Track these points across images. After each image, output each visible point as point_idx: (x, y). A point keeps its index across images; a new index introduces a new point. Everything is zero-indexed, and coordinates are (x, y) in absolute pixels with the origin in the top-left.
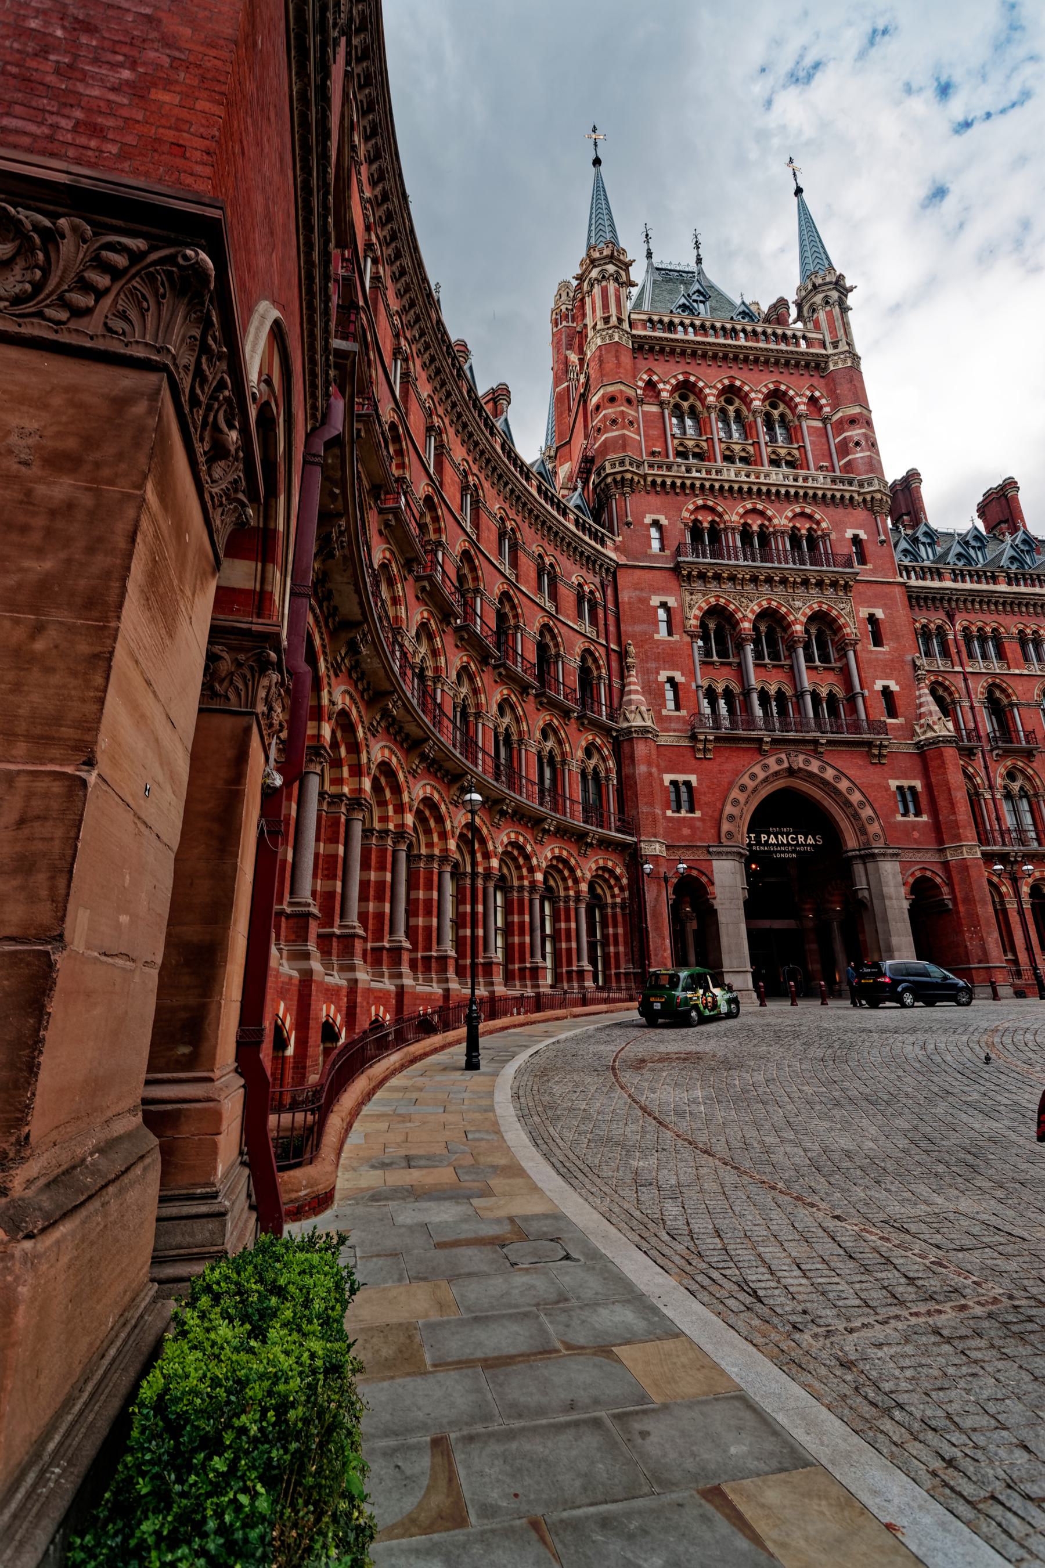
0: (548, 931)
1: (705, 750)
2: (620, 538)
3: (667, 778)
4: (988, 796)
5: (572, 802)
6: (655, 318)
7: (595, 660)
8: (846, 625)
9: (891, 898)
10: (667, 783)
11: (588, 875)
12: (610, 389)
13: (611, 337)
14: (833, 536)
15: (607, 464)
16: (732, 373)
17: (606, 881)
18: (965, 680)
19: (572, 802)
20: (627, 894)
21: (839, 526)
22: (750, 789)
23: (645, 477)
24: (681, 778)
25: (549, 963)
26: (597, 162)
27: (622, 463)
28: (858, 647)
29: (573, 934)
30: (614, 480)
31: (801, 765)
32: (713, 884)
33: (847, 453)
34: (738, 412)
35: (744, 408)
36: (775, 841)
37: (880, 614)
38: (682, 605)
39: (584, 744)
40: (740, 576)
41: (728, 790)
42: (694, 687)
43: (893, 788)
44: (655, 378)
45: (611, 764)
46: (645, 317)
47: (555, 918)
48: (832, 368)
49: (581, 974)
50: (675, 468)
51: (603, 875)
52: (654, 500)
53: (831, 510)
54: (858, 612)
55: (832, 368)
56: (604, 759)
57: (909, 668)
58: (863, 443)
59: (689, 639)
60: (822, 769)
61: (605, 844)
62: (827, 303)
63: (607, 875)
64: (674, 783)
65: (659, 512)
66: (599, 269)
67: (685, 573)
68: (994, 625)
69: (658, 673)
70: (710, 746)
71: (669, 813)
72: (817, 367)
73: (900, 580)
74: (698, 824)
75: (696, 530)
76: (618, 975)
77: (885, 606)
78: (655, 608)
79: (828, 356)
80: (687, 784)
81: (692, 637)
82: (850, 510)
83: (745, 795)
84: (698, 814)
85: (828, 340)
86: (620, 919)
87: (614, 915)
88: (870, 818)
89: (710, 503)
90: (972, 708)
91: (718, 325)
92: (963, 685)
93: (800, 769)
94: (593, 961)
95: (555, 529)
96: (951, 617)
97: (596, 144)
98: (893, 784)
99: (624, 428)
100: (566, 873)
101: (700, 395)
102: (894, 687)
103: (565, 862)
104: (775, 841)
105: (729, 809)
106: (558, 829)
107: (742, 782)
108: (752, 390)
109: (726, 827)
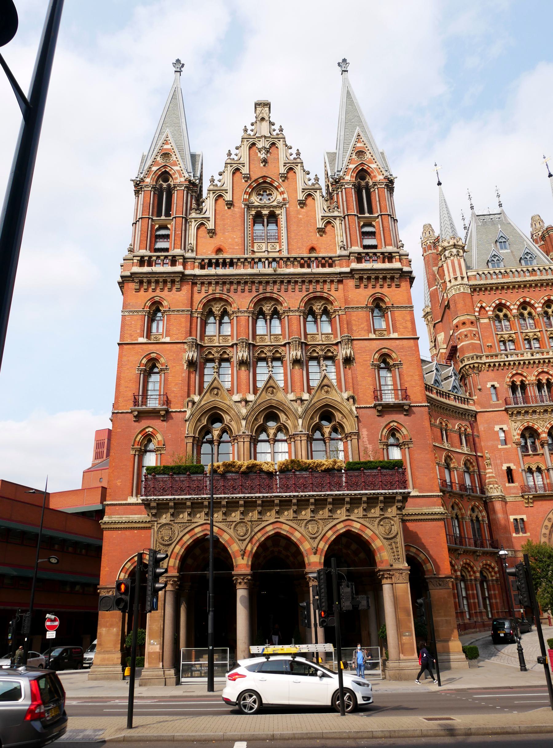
0: (464, 595)
2: (476, 397)
3: (512, 518)
5: (469, 539)
6: (480, 273)
7: (471, 463)
10: (512, 520)
11: (479, 569)
12: (462, 318)
13: (459, 289)
15: (465, 359)
16: (524, 295)
17: (488, 569)
19: (469, 539)
20: (498, 575)
23: (485, 364)
24: (518, 517)
25: (466, 608)
26: (439, 184)
27: (472, 358)
29: (476, 596)
30: (470, 367)
34: (530, 314)
35: (532, 311)
38: (510, 429)
39: (470, 507)
42: (520, 471)
44: (484, 305)
45: (484, 513)
46: (475, 273)
47: (467, 589)
49: (481, 612)
51: (486, 567)
52: (491, 374)
56: (481, 512)
59: (515, 446)
61: (485, 553)
63: (488, 567)
64: (516, 520)
66: (449, 251)
67: (510, 413)
69: (502, 466)
75: (513, 387)
76: (497, 612)
78: (497, 433)
80: (522, 519)
84: (528, 534)
86: (496, 587)
87: (493, 585)
91: (514, 270)
94: (485, 606)
99: (472, 339)
100: (469, 569)
101: (508, 308)
103: (469, 564)
106: (464, 552)
108: (536, 302)
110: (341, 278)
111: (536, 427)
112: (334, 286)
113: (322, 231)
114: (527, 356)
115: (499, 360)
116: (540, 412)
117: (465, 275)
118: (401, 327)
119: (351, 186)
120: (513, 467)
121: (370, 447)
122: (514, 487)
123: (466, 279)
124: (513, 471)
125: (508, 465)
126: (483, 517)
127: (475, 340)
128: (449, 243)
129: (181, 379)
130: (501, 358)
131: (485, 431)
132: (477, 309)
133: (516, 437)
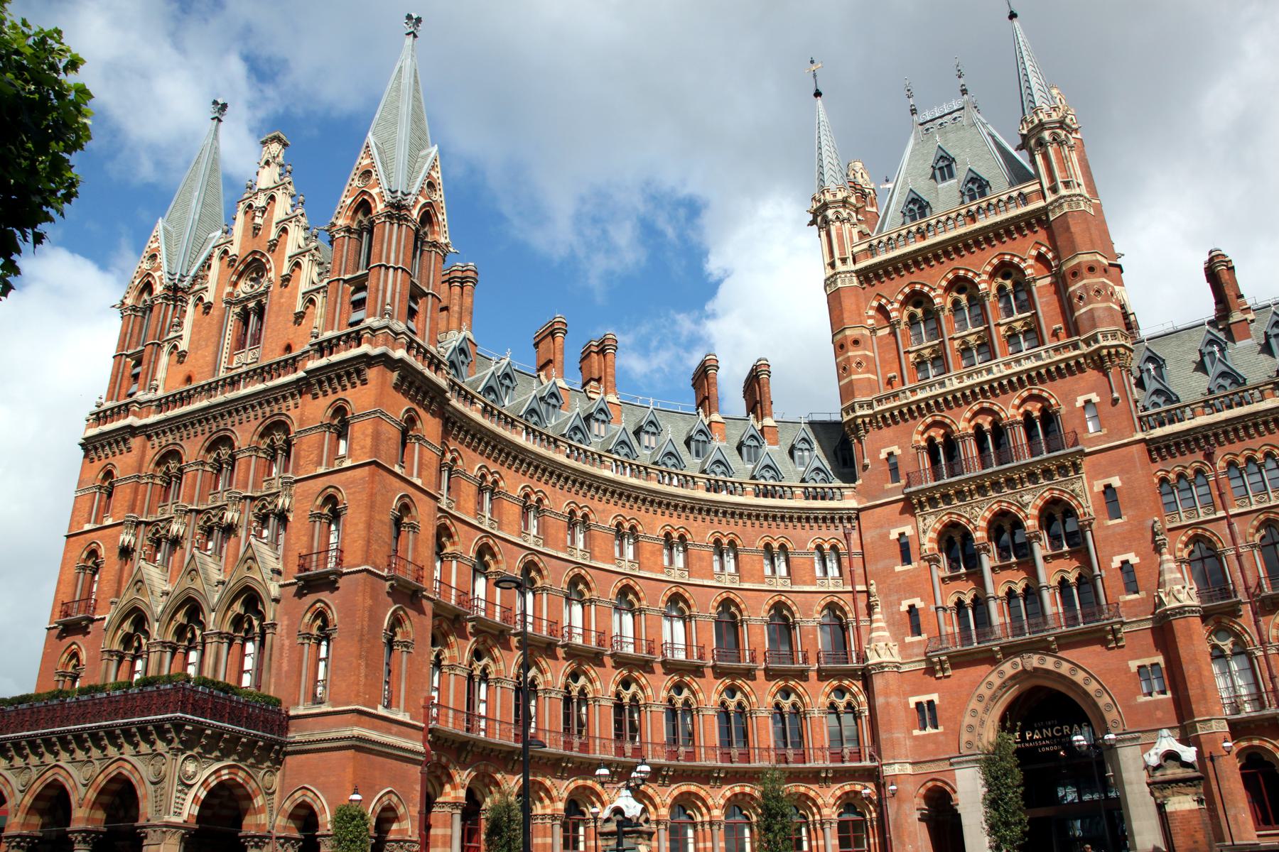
1: (943, 670)
3: (912, 701)
4: (1259, 653)
9: (1131, 783)
10: (912, 706)
18: (1230, 525)
22: (987, 697)
24: (924, 698)
28: (1093, 526)
32: (955, 792)
37: (1116, 482)
41: (965, 704)
42: (933, 608)
43: (1134, 669)
44: (883, 301)
45: (862, 698)
48: (1052, 219)
50: (901, 395)
53: (1059, 382)
54: (1091, 487)
57: (1149, 535)
59: (927, 563)
60: (1057, 664)
65: (893, 444)
68: (1266, 448)
69: (900, 604)
71: (916, 732)
73: (1139, 436)
74: (942, 738)
77: (1120, 473)
80: (930, 703)
81: (929, 561)
82: (1078, 375)
83: (983, 704)
84: (941, 729)
85: (1046, 184)
88: (1108, 705)
89: (938, 418)
90: (1238, 556)
92: (1228, 531)
93: (1035, 669)
95: (779, 514)
96: (1209, 456)
97: (815, 76)
98: (1134, 665)
102: (1133, 559)
105: (967, 720)
107: (979, 692)
109: (965, 737)
110: (302, 387)
112: (291, 403)
113: (299, 317)
118: (358, 448)
119: (342, 234)
120: (919, 603)
121: (287, 642)
122: (920, 641)
123: (850, 261)
124: (920, 612)
125: (910, 602)
128: (835, 195)
129: (113, 573)
131: (872, 543)
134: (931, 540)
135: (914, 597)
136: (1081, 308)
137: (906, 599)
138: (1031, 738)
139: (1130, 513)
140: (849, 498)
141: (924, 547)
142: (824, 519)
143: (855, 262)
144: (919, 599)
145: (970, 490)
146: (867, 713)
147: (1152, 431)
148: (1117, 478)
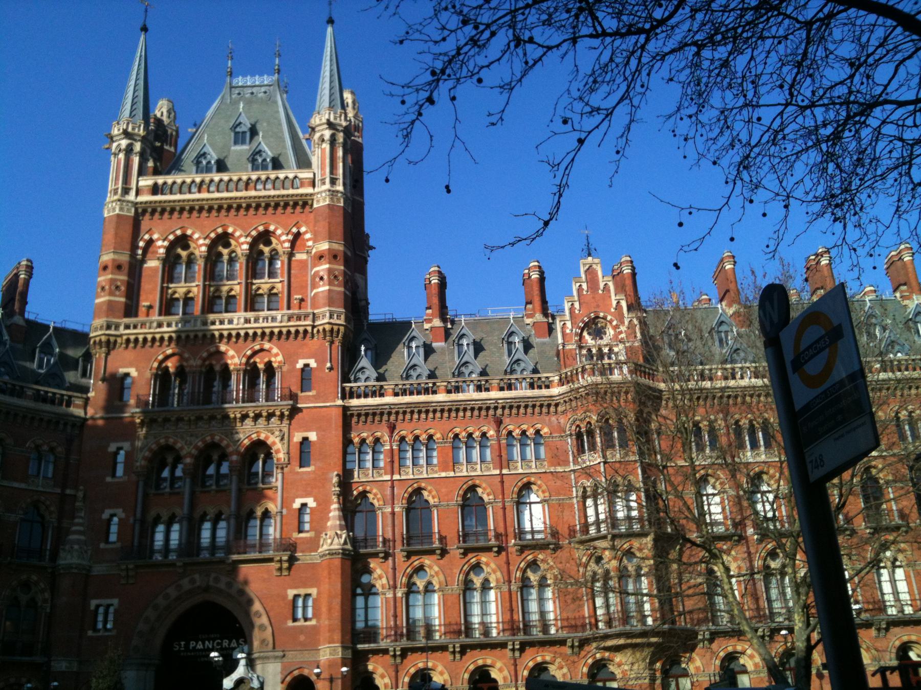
8: (278, 451)
13: (114, 209)
14: (285, 369)
21: (290, 359)
23: (121, 336)
31: (211, 583)
33: (314, 286)
36: (201, 647)
40: (186, 418)
42: (131, 520)
45: (47, 595)
52: (130, 354)
55: (315, 206)
58: (325, 277)
62: (323, 141)
69: (103, 512)
70: (131, 573)
72: (305, 204)
77: (318, 430)
79: (311, 195)
90: (393, 513)
96: (392, 428)
97: (146, 11)
104: (201, 647)
111: (179, 445)
114: (195, 326)
115: (146, 331)
116: (190, 420)
117: (134, 185)
123: (133, 193)
126: (45, 601)
127: (115, 296)
130: (150, 328)
132: (141, 244)
133: (138, 464)
134: (145, 458)
135: (117, 508)
136: (320, 286)
137: (110, 508)
138: (194, 648)
139: (319, 464)
140: (77, 406)
141: (138, 464)
142: (49, 422)
143: (137, 194)
144: (121, 510)
145: (190, 420)
146: (48, 610)
147: (351, 401)
148: (314, 433)
